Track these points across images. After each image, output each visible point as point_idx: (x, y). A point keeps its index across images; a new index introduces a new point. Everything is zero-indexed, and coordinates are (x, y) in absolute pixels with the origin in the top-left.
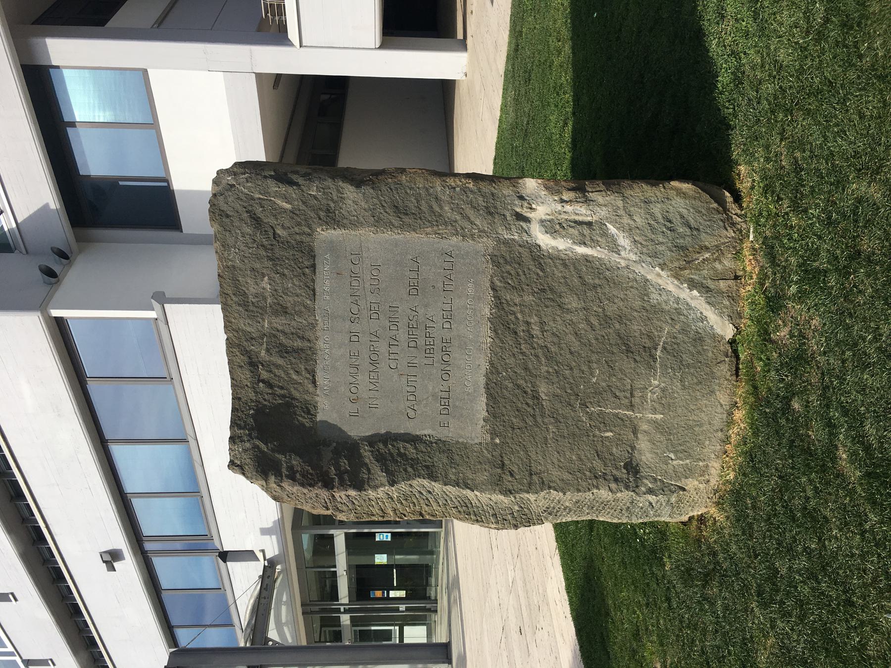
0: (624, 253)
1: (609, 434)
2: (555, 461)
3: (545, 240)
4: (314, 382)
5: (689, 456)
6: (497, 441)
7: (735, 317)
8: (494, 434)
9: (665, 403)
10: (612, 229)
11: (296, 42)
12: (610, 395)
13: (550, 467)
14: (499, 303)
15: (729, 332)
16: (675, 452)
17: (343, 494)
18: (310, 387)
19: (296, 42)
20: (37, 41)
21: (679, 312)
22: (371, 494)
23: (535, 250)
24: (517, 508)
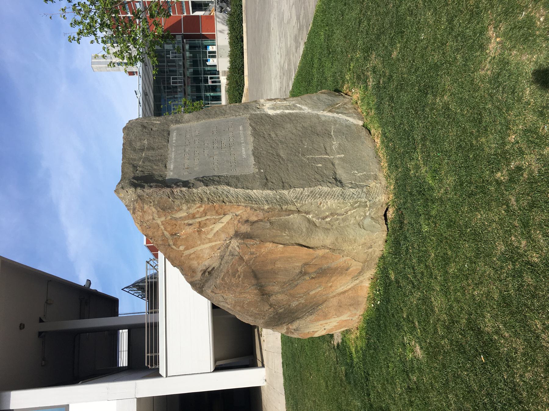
0: (306, 110)
1: (320, 165)
2: (295, 177)
3: (271, 112)
4: (166, 167)
5: (365, 171)
6: (262, 171)
7: (361, 119)
8: (260, 169)
9: (342, 149)
10: (298, 105)
11: (164, 375)
12: (315, 151)
13: (292, 180)
14: (254, 129)
15: (361, 123)
16: (357, 170)
17: (178, 189)
18: (164, 169)
19: (164, 375)
20: (7, 393)
21: (336, 121)
22: (195, 190)
23: (268, 116)
24: (278, 197)
